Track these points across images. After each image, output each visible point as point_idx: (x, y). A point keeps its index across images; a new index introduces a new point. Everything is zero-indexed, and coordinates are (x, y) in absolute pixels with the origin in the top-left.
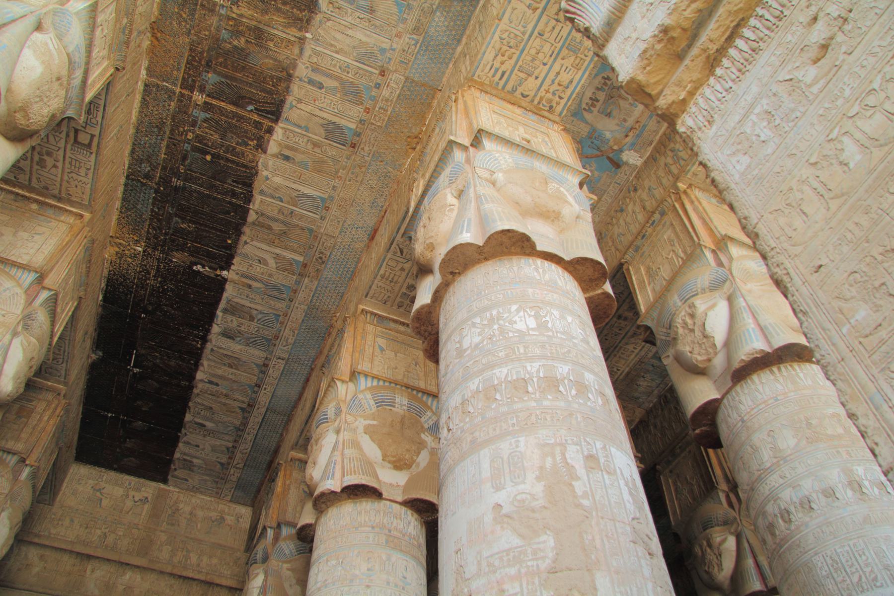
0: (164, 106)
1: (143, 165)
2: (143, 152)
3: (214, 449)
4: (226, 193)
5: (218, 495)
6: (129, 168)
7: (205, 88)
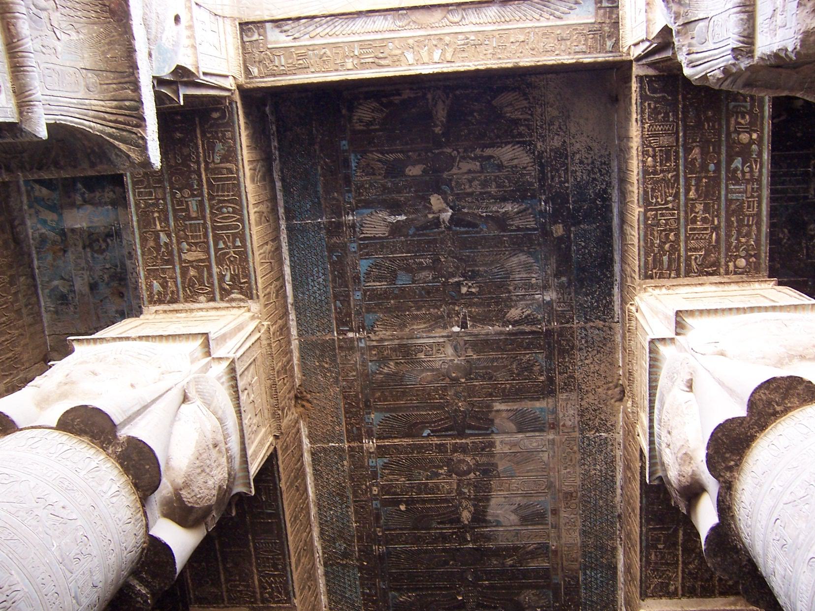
0: (338, 469)
1: (337, 544)
2: (333, 529)
4: (435, 540)
6: (324, 553)
7: (372, 431)
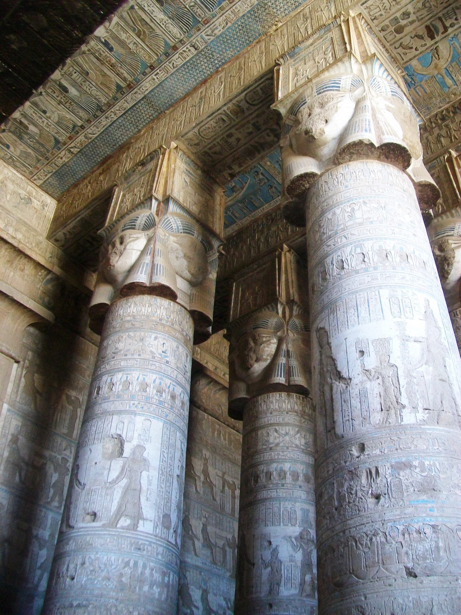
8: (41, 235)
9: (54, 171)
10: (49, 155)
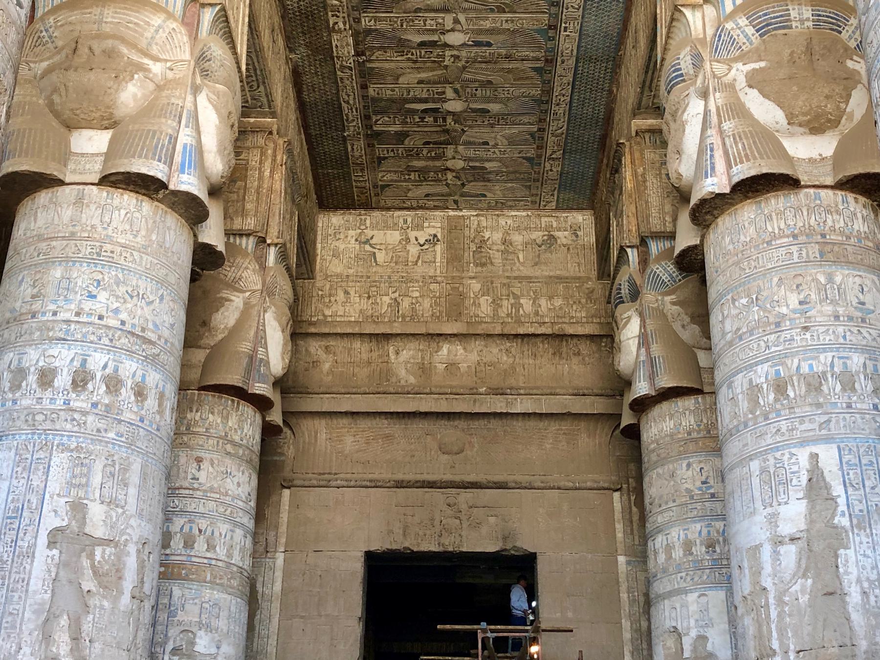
3: (512, 141)
5: (536, 205)
8: (589, 279)
9: (557, 186)
10: (533, 176)
